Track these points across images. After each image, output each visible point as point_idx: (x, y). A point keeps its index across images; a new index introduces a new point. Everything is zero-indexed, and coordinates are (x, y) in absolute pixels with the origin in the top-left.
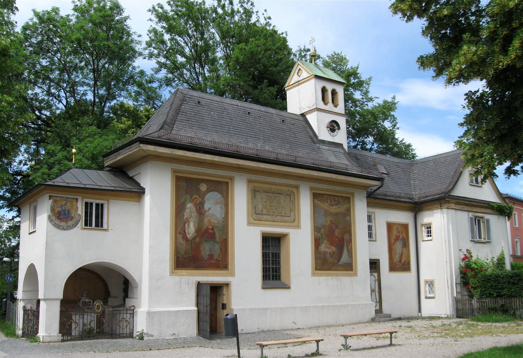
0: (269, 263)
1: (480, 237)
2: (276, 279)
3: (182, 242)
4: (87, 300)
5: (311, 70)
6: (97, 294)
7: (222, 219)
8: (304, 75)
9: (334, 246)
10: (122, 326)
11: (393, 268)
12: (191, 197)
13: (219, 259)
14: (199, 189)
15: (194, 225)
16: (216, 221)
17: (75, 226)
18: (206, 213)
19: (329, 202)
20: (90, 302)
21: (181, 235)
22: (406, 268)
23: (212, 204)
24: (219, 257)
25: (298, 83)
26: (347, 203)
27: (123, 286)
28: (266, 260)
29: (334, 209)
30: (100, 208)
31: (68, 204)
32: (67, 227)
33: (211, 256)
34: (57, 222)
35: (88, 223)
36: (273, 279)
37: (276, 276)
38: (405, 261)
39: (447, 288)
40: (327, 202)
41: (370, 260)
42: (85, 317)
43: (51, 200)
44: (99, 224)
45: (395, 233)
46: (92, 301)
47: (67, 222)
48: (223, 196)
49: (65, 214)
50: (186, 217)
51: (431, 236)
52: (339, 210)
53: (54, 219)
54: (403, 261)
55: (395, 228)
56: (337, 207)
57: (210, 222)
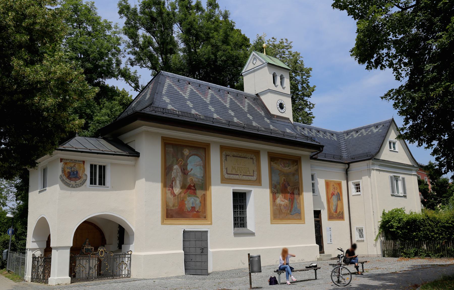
1: (398, 192)
2: (244, 227)
3: (170, 196)
4: (90, 248)
5: (264, 59)
6: (100, 241)
7: (201, 178)
8: (258, 63)
10: (121, 268)
11: (331, 217)
12: (177, 160)
13: (199, 211)
14: (183, 154)
15: (180, 183)
16: (196, 180)
17: (82, 185)
20: (92, 249)
21: (170, 191)
22: (340, 217)
25: (254, 71)
27: (118, 235)
28: (235, 211)
29: (287, 169)
30: (102, 169)
32: (76, 185)
33: (193, 208)
34: (68, 181)
35: (92, 182)
36: (241, 227)
38: (340, 212)
39: (374, 234)
41: (314, 211)
42: (91, 261)
43: (63, 163)
44: (102, 182)
45: (331, 188)
46: (93, 248)
47: (75, 181)
48: (202, 159)
49: (74, 174)
50: (173, 176)
51: (360, 191)
53: (65, 179)
55: (331, 185)
57: (192, 180)
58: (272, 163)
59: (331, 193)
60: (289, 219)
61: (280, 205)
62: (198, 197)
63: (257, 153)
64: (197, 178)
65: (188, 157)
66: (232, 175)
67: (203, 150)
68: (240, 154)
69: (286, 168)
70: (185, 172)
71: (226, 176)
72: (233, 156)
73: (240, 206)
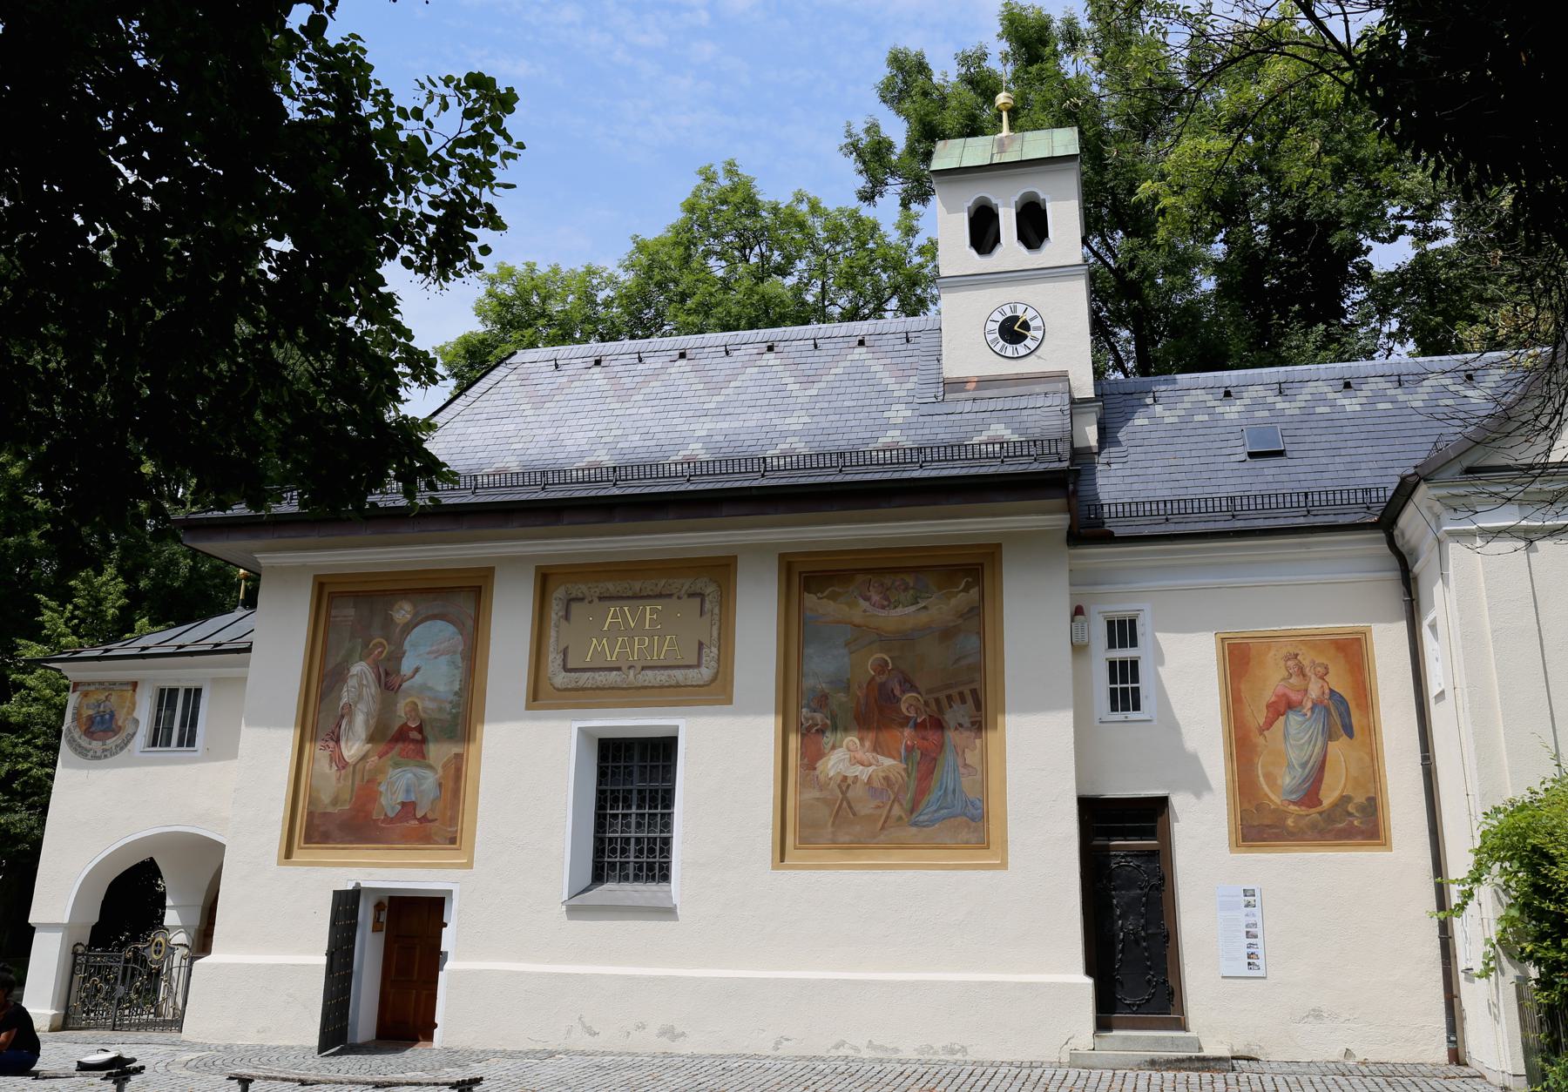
0: (628, 825)
7: (451, 697)
9: (890, 756)
11: (1257, 827)
12: (366, 645)
13: (430, 816)
14: (388, 622)
15: (367, 722)
16: (431, 705)
18: (405, 685)
19: (876, 598)
21: (327, 753)
22: (1360, 823)
23: (428, 658)
24: (432, 810)
26: (966, 589)
31: (113, 699)
33: (408, 807)
34: (84, 742)
36: (637, 878)
37: (651, 867)
38: (1345, 800)
40: (867, 599)
44: (188, 740)
45: (1272, 679)
47: (103, 740)
49: (103, 721)
50: (345, 700)
52: (924, 617)
53: (76, 736)
54: (1328, 797)
56: (913, 608)
58: (810, 599)
59: (1269, 696)
60: (901, 845)
61: (845, 783)
62: (430, 767)
63: (719, 572)
64: (434, 699)
65: (408, 628)
66: (588, 674)
67: (466, 594)
68: (637, 586)
69: (900, 611)
70: (389, 681)
71: (561, 679)
72: (600, 599)
73: (640, 792)
